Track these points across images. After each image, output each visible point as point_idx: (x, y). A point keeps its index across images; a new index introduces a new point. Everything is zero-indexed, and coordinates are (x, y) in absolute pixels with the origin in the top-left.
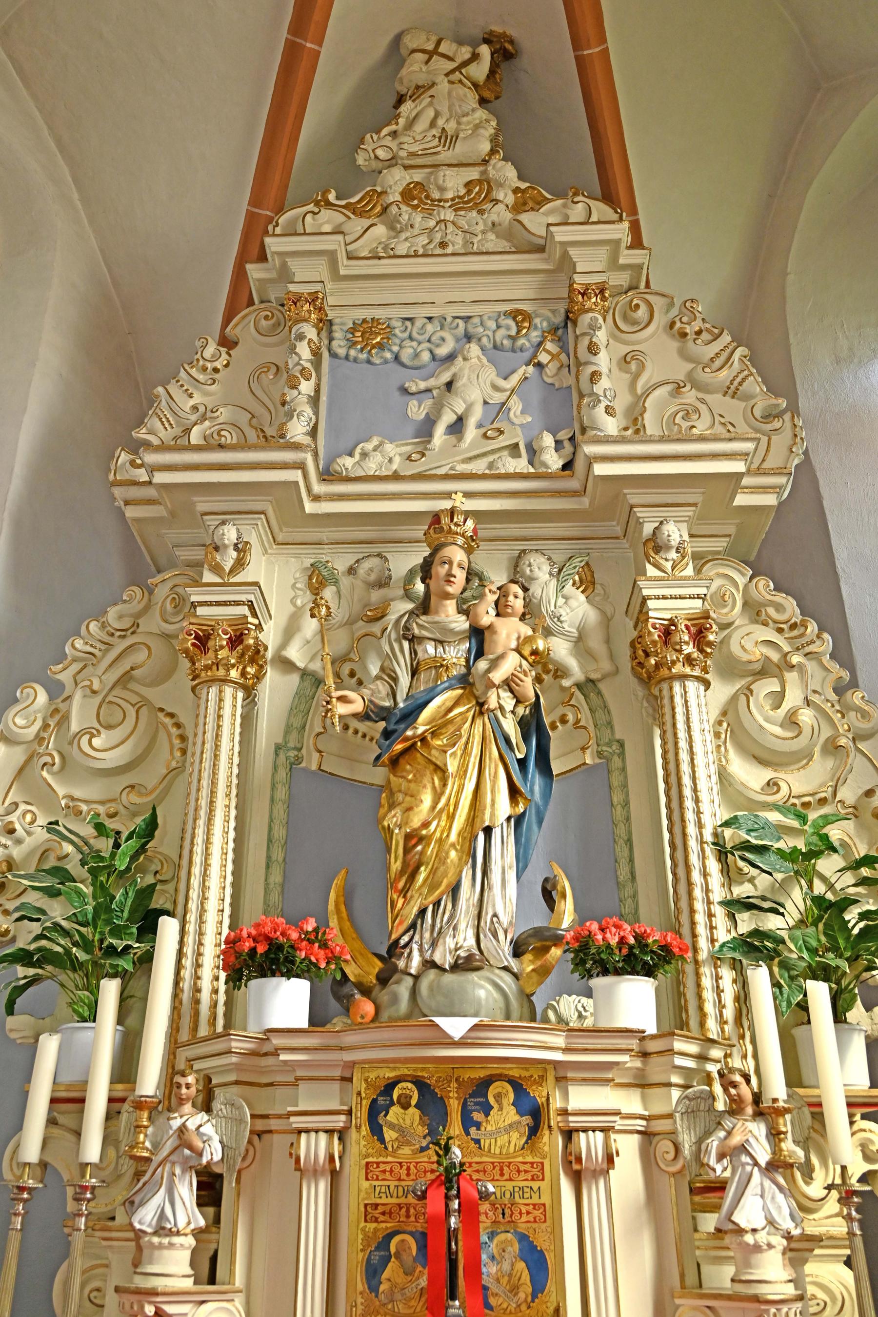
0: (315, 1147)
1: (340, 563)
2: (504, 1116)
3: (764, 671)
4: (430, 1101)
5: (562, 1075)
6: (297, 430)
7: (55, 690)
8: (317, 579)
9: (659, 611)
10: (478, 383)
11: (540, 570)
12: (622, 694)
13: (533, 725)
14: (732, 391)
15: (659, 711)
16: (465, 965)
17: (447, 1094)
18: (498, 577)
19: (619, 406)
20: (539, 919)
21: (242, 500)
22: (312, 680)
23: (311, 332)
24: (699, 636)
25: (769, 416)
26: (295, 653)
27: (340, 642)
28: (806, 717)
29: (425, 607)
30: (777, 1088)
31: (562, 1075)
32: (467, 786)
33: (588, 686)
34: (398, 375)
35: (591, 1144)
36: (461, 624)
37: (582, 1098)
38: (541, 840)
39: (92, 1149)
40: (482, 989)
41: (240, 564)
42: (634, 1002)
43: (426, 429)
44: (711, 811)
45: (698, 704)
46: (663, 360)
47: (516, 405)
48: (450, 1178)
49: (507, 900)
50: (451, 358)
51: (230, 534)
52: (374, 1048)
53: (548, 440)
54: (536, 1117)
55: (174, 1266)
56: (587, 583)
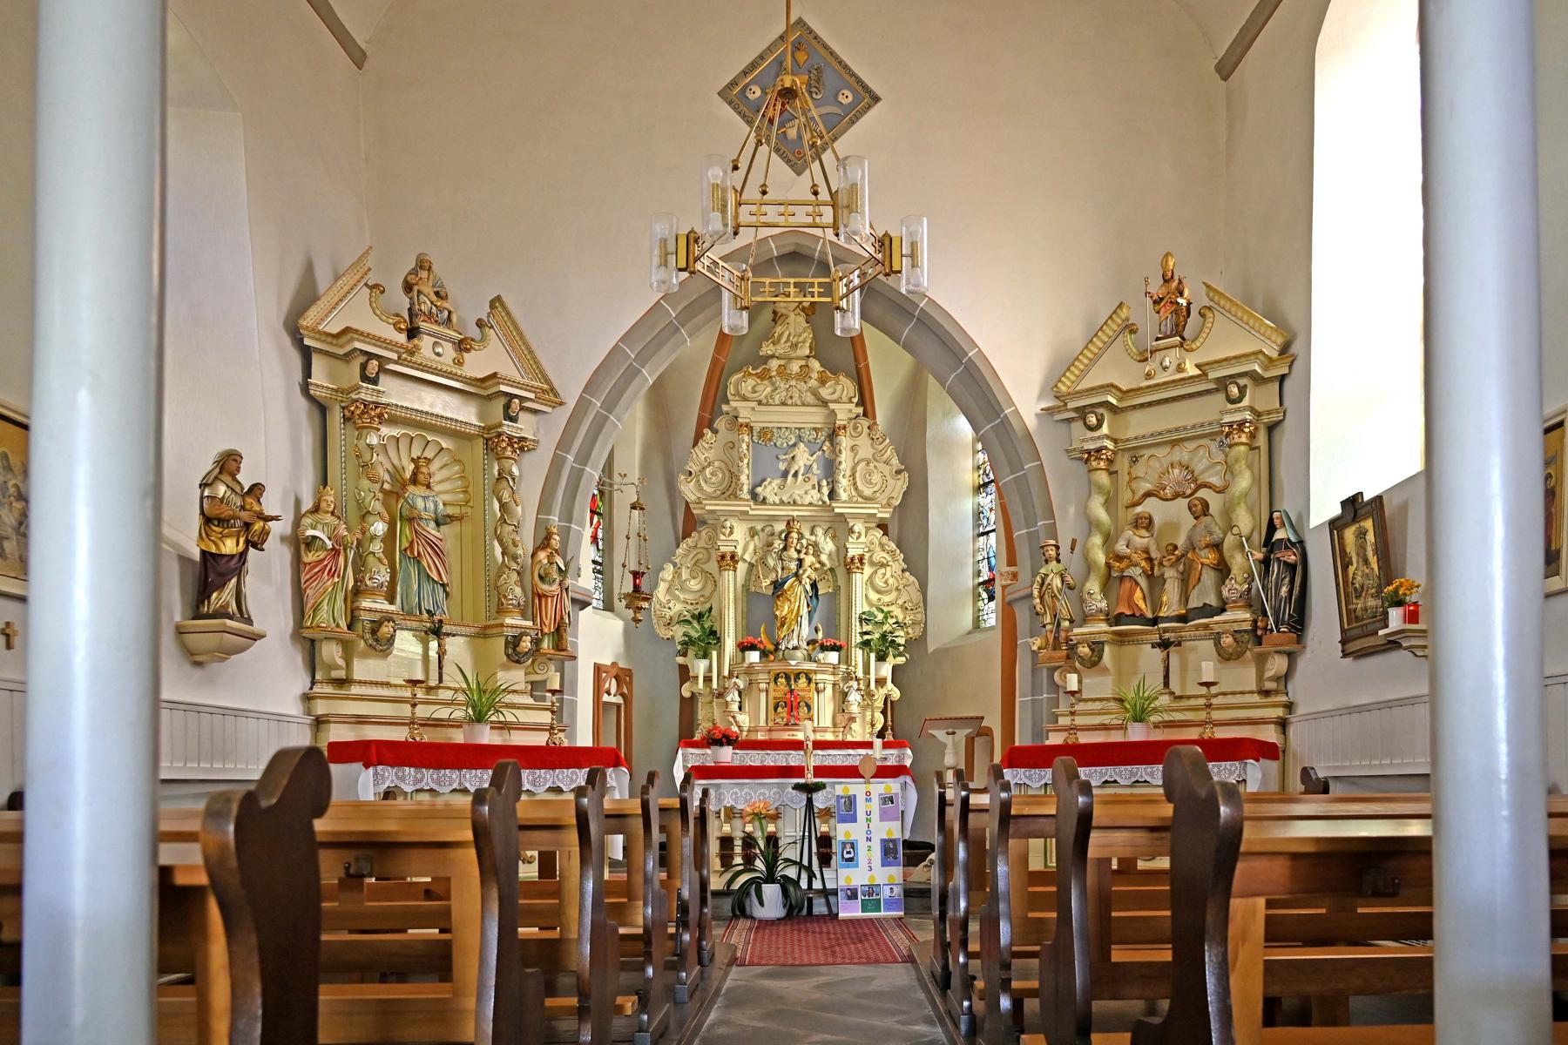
0: (763, 686)
1: (759, 527)
2: (803, 680)
3: (883, 565)
4: (787, 677)
5: (815, 672)
6: (743, 478)
7: (675, 565)
8: (753, 533)
9: (850, 555)
10: (803, 457)
11: (819, 531)
12: (841, 573)
13: (814, 586)
14: (887, 463)
15: (849, 581)
16: (795, 648)
17: (791, 677)
18: (807, 534)
19: (848, 473)
20: (813, 637)
21: (732, 514)
22: (751, 565)
23: (746, 438)
24: (861, 559)
25: (898, 472)
26: (747, 557)
27: (760, 553)
28: (891, 581)
29: (785, 549)
30: (860, 674)
31: (815, 672)
32: (797, 602)
33: (831, 570)
34: (776, 451)
35: (821, 686)
36: (795, 555)
37: (819, 676)
38: (816, 616)
39: (715, 685)
40: (799, 654)
41: (731, 533)
42: (833, 657)
43: (785, 474)
44: (860, 607)
45: (859, 579)
46: (866, 451)
47: (815, 466)
48: (792, 691)
49: (806, 631)
50: (795, 445)
51: (728, 524)
52: (776, 667)
53: (824, 483)
54: (809, 680)
55: (735, 707)
56: (834, 538)
